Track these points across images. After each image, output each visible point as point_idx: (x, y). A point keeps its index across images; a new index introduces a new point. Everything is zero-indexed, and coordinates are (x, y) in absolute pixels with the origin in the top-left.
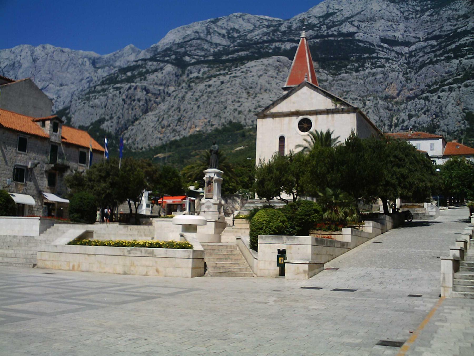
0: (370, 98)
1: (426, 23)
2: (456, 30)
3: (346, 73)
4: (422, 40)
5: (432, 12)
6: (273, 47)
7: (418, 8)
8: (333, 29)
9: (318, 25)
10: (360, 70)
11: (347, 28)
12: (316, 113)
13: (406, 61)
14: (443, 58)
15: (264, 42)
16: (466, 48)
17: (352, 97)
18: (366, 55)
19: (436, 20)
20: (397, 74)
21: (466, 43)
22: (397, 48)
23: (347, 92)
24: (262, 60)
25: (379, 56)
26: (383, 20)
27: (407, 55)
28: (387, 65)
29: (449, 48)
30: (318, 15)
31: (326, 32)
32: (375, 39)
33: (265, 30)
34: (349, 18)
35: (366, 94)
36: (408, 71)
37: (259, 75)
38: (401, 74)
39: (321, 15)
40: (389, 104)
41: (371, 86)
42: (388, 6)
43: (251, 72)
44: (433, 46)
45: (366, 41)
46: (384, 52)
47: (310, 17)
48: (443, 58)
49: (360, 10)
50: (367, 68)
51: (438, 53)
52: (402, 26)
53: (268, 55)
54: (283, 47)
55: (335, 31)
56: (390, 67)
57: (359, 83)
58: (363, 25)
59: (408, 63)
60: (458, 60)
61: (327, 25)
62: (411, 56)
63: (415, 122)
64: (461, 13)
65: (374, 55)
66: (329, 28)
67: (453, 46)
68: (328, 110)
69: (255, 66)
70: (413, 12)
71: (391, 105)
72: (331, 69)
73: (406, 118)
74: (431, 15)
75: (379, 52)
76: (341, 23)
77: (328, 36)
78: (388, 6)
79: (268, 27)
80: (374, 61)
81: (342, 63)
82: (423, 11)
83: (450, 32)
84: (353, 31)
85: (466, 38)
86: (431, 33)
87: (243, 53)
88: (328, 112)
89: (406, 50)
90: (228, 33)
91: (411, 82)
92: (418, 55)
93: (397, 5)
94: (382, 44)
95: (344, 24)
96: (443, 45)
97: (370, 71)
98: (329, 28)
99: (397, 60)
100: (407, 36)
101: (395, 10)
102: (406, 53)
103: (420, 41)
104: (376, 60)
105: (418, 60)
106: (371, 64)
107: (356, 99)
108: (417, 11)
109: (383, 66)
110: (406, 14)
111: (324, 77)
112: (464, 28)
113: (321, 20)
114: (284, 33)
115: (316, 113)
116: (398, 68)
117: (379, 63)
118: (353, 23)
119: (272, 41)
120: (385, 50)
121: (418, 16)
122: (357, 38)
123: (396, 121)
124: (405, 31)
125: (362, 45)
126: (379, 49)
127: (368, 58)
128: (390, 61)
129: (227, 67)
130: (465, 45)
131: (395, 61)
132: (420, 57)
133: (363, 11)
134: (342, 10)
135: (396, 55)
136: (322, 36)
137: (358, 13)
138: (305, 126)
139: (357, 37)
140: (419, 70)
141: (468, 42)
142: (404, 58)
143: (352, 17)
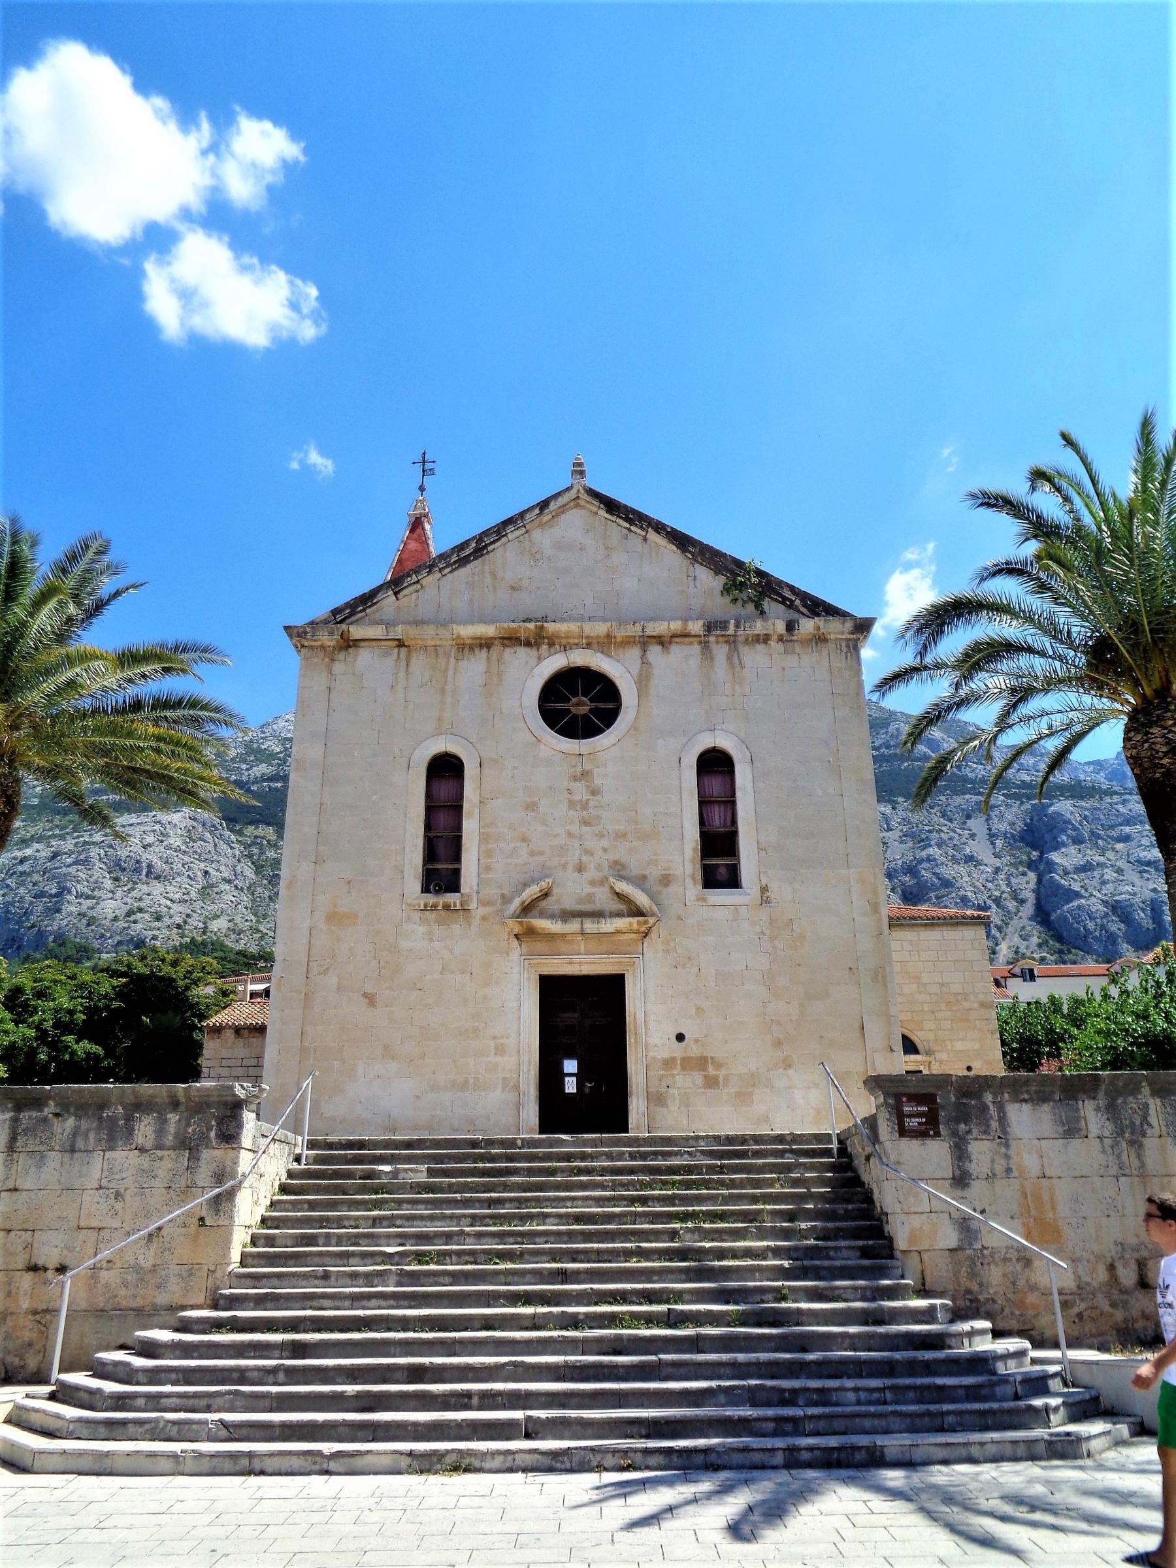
47: (265, 738)
138: (581, 706)
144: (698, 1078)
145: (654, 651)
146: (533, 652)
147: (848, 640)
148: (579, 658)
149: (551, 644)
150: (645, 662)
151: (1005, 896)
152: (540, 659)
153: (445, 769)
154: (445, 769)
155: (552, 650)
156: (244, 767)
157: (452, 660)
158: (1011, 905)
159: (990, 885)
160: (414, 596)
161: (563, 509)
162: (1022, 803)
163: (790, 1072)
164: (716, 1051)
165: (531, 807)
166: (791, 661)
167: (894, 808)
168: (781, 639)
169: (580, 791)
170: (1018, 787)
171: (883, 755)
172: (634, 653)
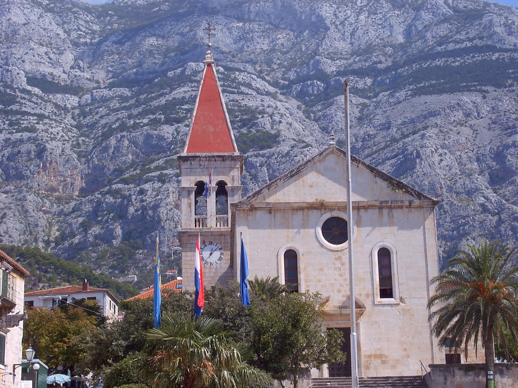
0: (8, 188)
4: (103, 86)
5: (120, 37)
7: (96, 28)
13: (75, 123)
14: (145, 121)
20: (60, 144)
21: (183, 98)
25: (24, 109)
27: (77, 111)
28: (40, 127)
29: (155, 103)
36: (81, 142)
38: (68, 146)
40: (45, 200)
42: (41, 16)
44: (123, 99)
46: (32, 102)
48: (145, 121)
51: (135, 112)
56: (46, 131)
59: (79, 127)
60: (173, 128)
62: (84, 114)
65: (15, 107)
67: (163, 101)
68: (381, 202)
70: (87, 34)
71: (48, 204)
75: (23, 101)
78: (41, 16)
80: (14, 118)
83: (155, 75)
89: (73, 101)
92: (97, 113)
93: (58, 18)
94: (29, 88)
96: (142, 97)
99: (58, 119)
100: (76, 76)
101: (54, 27)
104: (19, 116)
105: (97, 122)
106: (10, 125)
108: (94, 32)
109: (32, 130)
110: (74, 35)
117: (25, 124)
120: (34, 99)
126: (23, 95)
128: (46, 121)
131: (55, 120)
132: (102, 117)
135: (55, 110)
140: (102, 140)
144: (379, 361)
145: (362, 211)
146: (319, 212)
147: (430, 207)
148: (336, 214)
149: (325, 209)
152: (322, 215)
155: (326, 211)
157: (290, 215)
160: (275, 190)
161: (327, 155)
163: (409, 359)
164: (385, 353)
165: (321, 270)
167: (484, 97)
168: (407, 207)
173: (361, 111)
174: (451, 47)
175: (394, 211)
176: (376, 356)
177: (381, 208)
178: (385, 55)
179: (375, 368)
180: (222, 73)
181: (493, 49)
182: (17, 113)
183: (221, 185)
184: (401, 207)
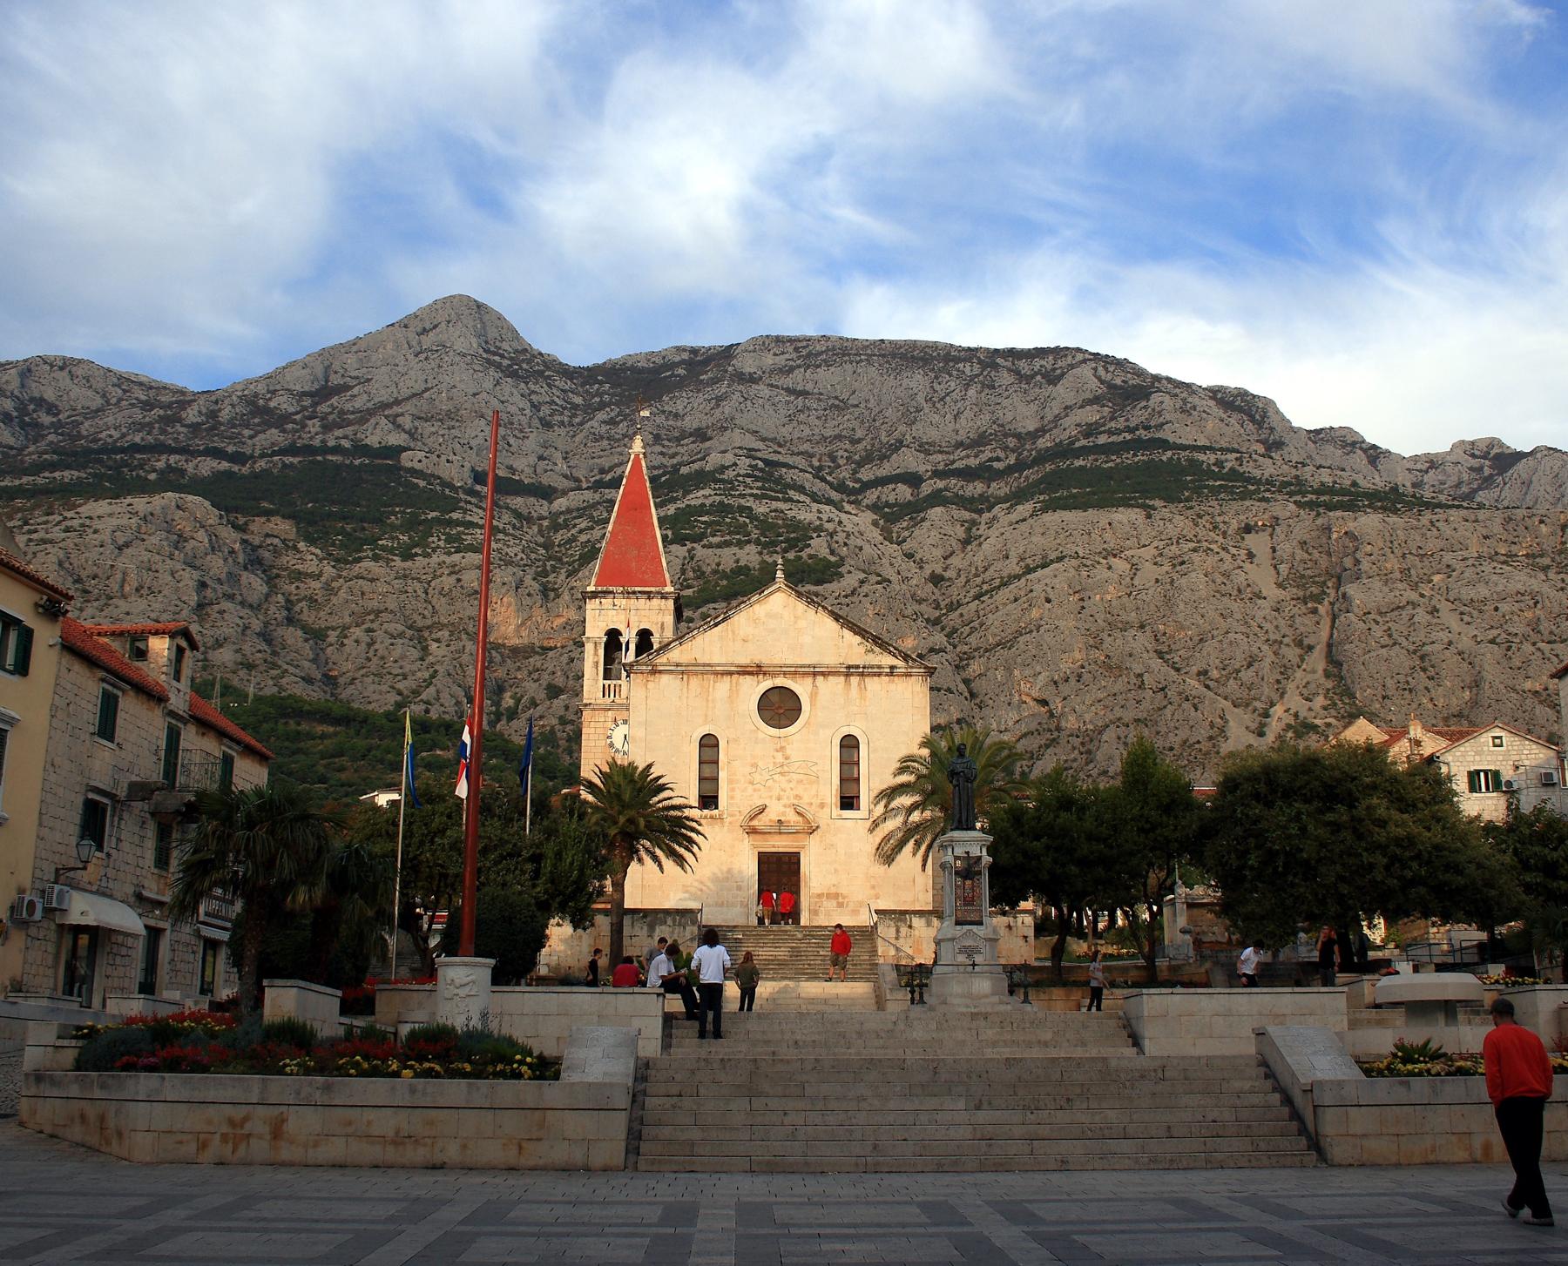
1: (597, 441)
2: (676, 468)
3: (376, 558)
4: (584, 485)
6: (160, 465)
7: (578, 400)
8: (339, 433)
9: (298, 417)
10: (416, 554)
11: (378, 434)
12: (815, 672)
15: (136, 448)
16: (705, 519)
17: (391, 627)
18: (433, 514)
19: (625, 436)
21: (703, 505)
22: (518, 502)
23: (378, 613)
24: (129, 500)
25: (468, 518)
26: (483, 422)
27: (545, 523)
30: (298, 388)
31: (320, 437)
32: (456, 472)
33: (138, 415)
34: (389, 406)
35: (429, 622)
37: (121, 543)
38: (531, 571)
39: (307, 389)
41: (443, 600)
43: (96, 532)
45: (432, 475)
47: (274, 392)
49: (419, 387)
50: (434, 550)
52: (532, 443)
53: (145, 488)
54: (190, 468)
55: (346, 437)
57: (410, 589)
58: (427, 428)
59: (547, 546)
61: (322, 419)
62: (556, 527)
63: (567, 708)
64: (690, 423)
65: (455, 515)
66: (327, 428)
68: (849, 667)
69: (110, 515)
72: (333, 545)
73: (542, 695)
74: (612, 422)
76: (365, 416)
77: (325, 450)
79: (147, 406)
81: (364, 529)
82: (590, 410)
84: (396, 443)
85: (702, 492)
86: (611, 469)
87: (68, 475)
88: (849, 671)
89: (541, 508)
90: (22, 410)
91: (558, 596)
93: (523, 385)
95: (373, 421)
97: (444, 558)
98: (327, 428)
99: (517, 533)
101: (517, 398)
102: (541, 518)
103: (579, 488)
105: (574, 539)
107: (401, 635)
108: (575, 407)
110: (545, 410)
111: (312, 566)
112: (696, 466)
113: (307, 402)
114: (195, 428)
115: (815, 672)
116: (521, 555)
117: (468, 540)
118: (400, 420)
119: (159, 449)
121: (577, 420)
122: (409, 465)
123: (511, 702)
124: (541, 458)
125: (422, 483)
127: (437, 520)
128: (501, 536)
129: (19, 510)
130: (701, 510)
131: (515, 537)
132: (581, 531)
133: (427, 390)
134: (369, 380)
136: (309, 450)
137: (415, 395)
139: (407, 459)
140: (581, 565)
141: (708, 502)
142: (535, 529)
143: (397, 402)
144: (834, 903)
145: (820, 679)
148: (780, 681)
150: (814, 685)
151: (1286, 640)
153: (709, 744)
154: (709, 744)
156: (247, 432)
158: (1292, 653)
159: (1267, 626)
162: (1318, 514)
164: (843, 891)
166: (892, 687)
167: (1149, 516)
169: (779, 757)
170: (1318, 492)
171: (1139, 440)
172: (809, 680)
173: (969, 530)
174: (1102, 439)
175: (867, 679)
176: (829, 896)
177: (848, 675)
178: (1005, 448)
179: (828, 914)
180: (761, 470)
181: (1164, 444)
182: (458, 523)
183: (644, 636)
184: (879, 675)
